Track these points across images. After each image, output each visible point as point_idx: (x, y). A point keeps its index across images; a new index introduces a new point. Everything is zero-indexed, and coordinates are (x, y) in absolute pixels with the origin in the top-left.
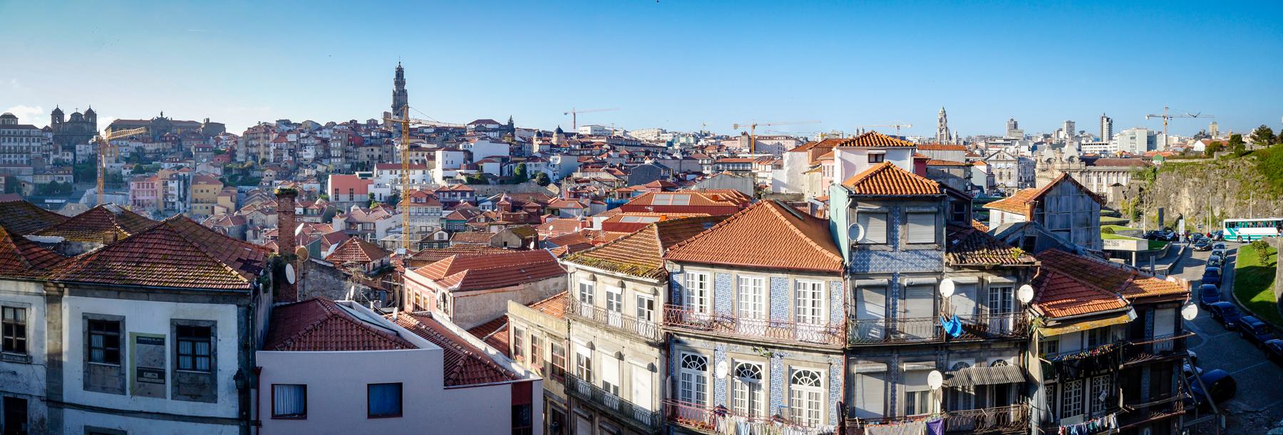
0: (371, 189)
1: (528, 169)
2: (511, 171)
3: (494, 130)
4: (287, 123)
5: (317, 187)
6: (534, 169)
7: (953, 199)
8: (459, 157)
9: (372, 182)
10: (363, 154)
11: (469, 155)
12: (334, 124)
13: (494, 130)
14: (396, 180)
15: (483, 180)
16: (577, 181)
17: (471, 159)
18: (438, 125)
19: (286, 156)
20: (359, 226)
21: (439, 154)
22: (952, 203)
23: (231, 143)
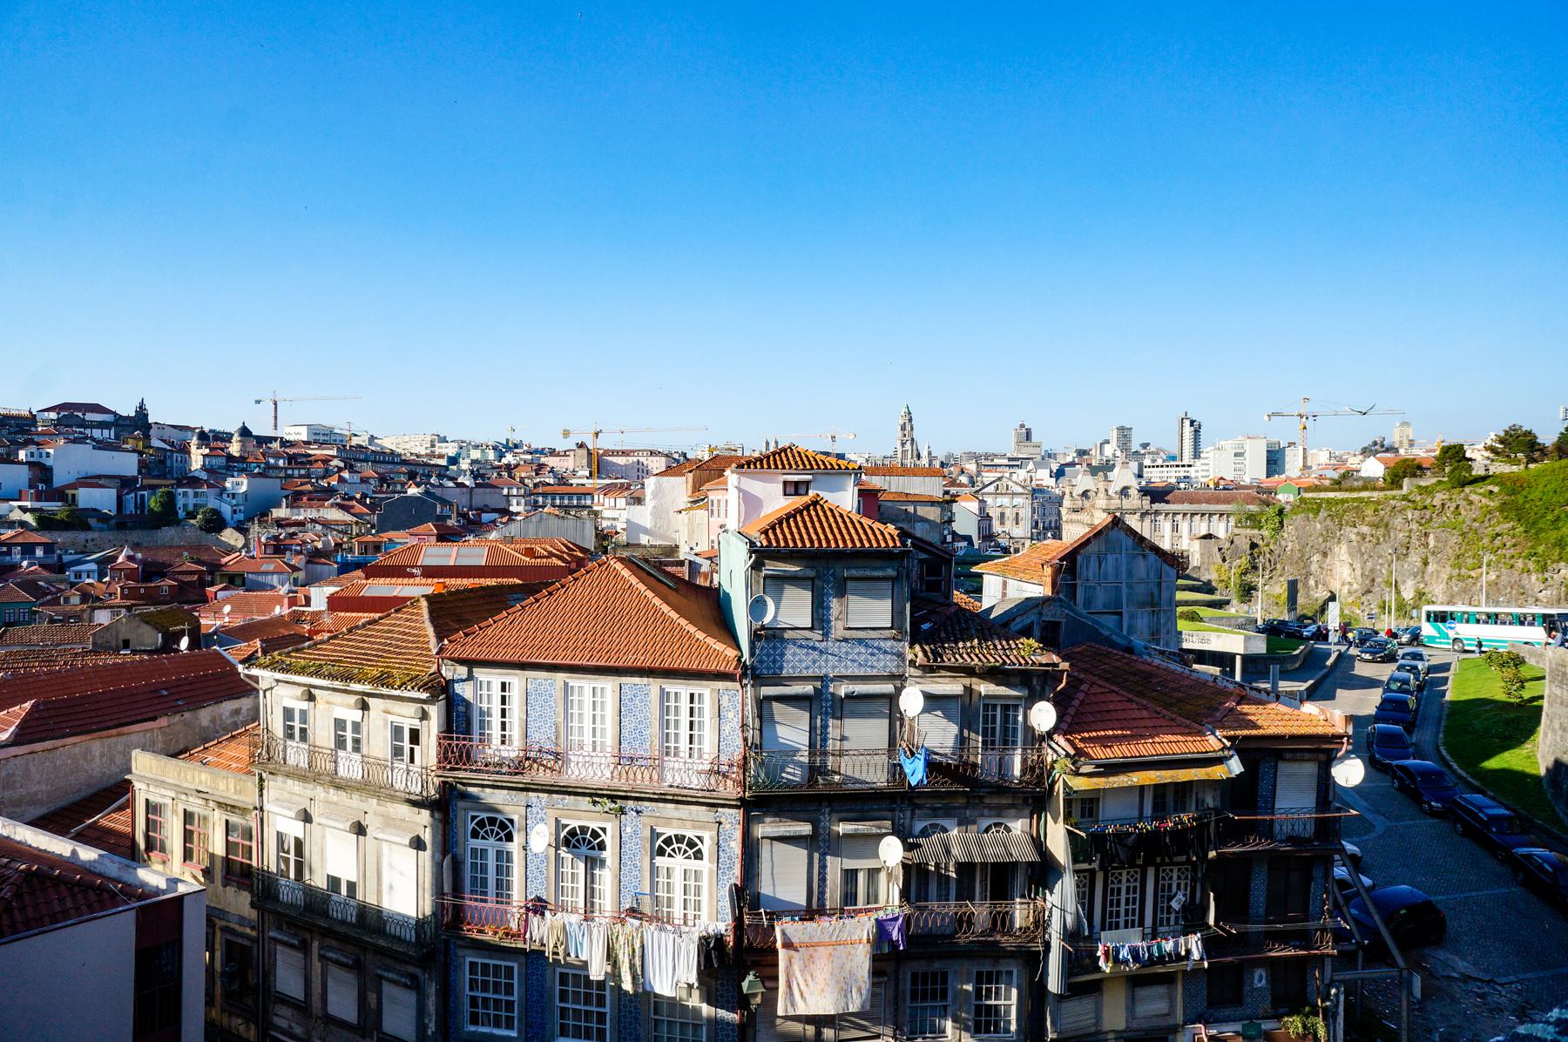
1: (180, 502)
3: (102, 425)
6: (191, 501)
7: (923, 556)
11: (41, 472)
13: (102, 425)
15: (79, 520)
16: (280, 523)
22: (921, 561)
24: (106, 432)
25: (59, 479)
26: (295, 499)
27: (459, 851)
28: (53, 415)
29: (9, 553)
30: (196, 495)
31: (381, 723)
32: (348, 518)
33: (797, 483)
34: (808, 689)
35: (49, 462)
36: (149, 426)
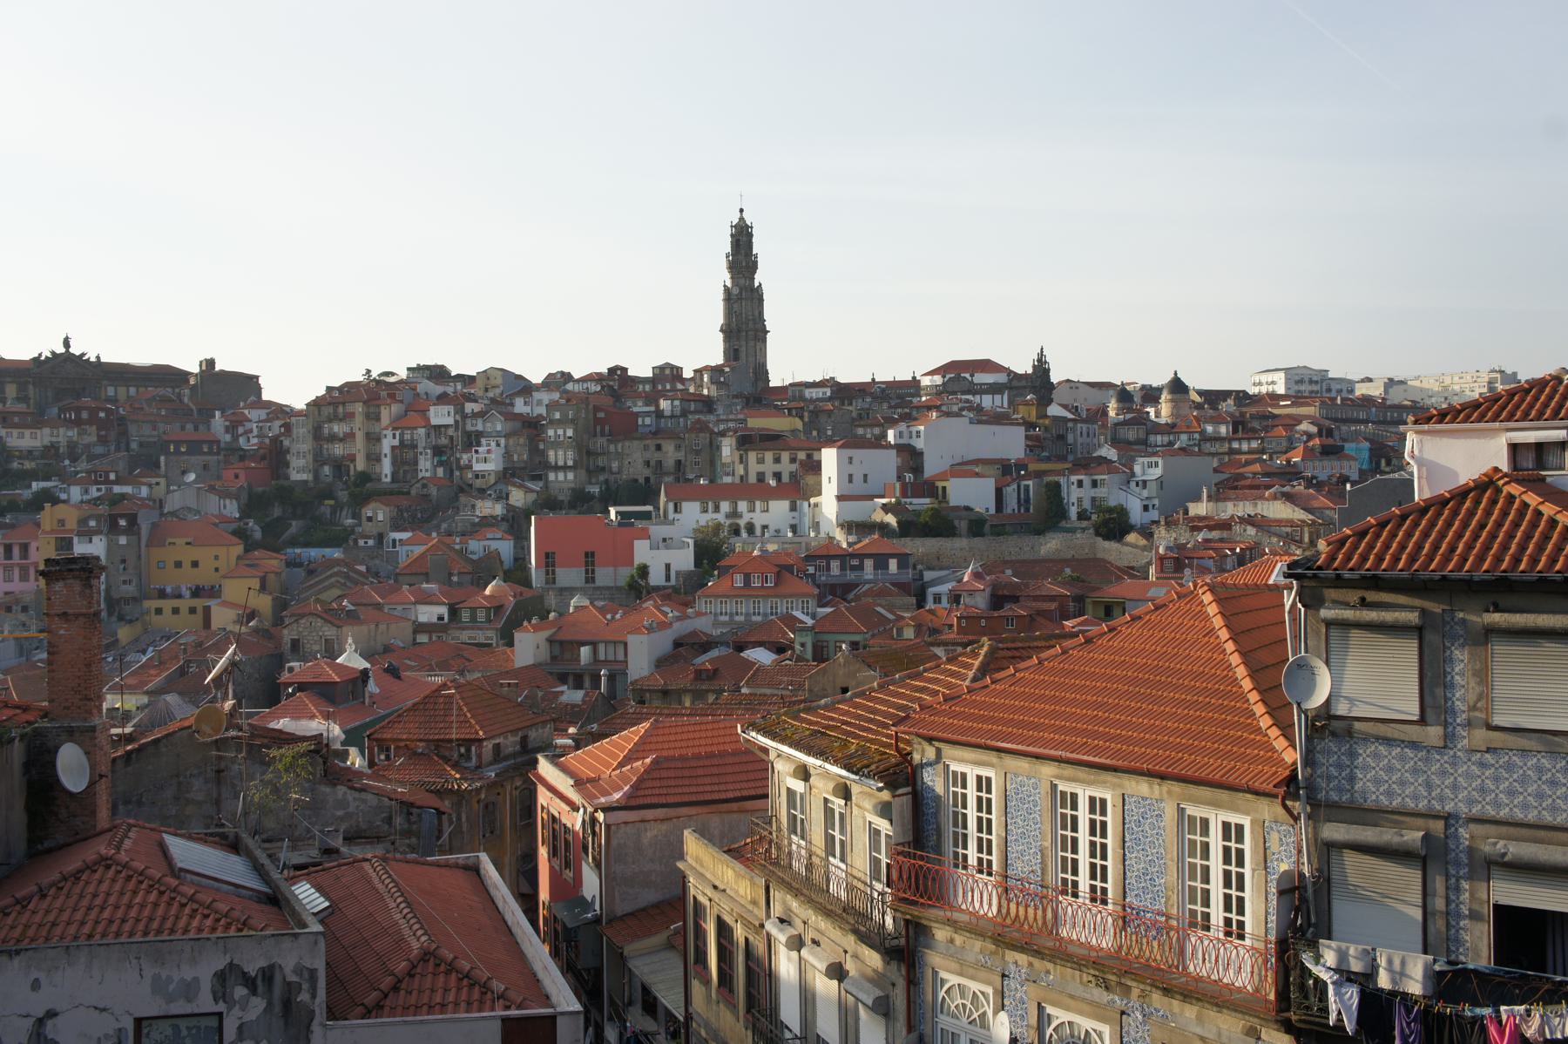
0: (642, 552)
2: (1024, 502)
3: (994, 389)
4: (438, 373)
5: (505, 548)
6: (1087, 493)
8: (884, 465)
9: (645, 535)
10: (632, 461)
11: (911, 457)
12: (566, 377)
13: (994, 389)
14: (718, 527)
15: (940, 524)
16: (1196, 524)
17: (918, 469)
18: (843, 379)
19: (425, 465)
20: (585, 651)
21: (829, 458)
23: (276, 427)
24: (997, 397)
25: (930, 470)
26: (1227, 487)
27: (927, 1031)
28: (938, 380)
29: (861, 567)
30: (1095, 484)
31: (860, 822)
32: (1299, 515)
33: (1540, 447)
34: (1413, 837)
35: (919, 444)
36: (1051, 387)
